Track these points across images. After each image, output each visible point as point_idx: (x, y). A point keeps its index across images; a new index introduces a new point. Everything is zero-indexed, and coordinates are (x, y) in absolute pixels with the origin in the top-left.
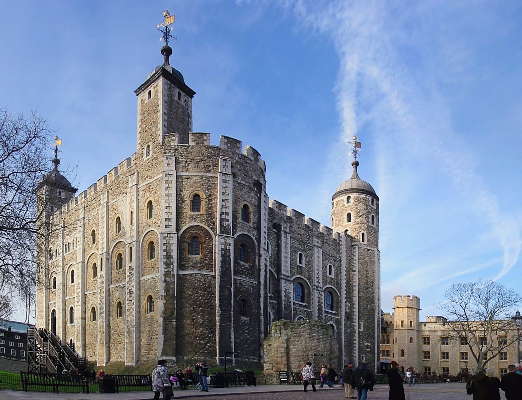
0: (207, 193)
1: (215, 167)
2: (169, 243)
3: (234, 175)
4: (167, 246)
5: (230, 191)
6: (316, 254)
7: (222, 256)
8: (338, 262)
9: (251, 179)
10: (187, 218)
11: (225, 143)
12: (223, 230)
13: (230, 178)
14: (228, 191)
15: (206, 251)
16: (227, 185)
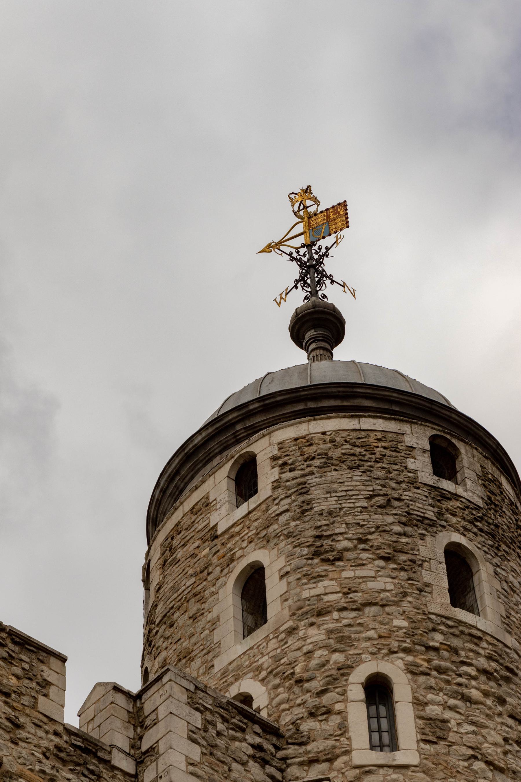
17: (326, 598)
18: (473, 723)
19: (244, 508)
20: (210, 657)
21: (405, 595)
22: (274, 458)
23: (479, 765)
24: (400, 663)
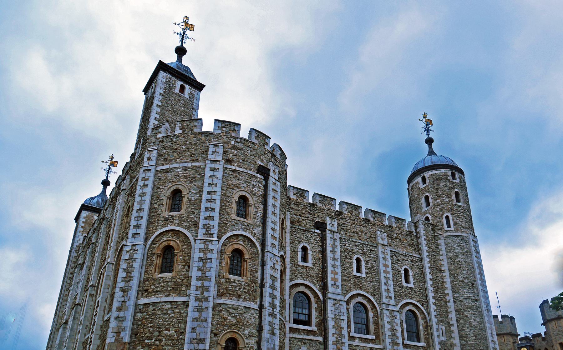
4: (129, 263)
6: (381, 256)
8: (417, 262)
9: (254, 164)
13: (220, 165)
14: (215, 181)
16: (216, 174)
17: (439, 203)
18: (461, 221)
19: (424, 186)
20: (421, 209)
21: (450, 202)
22: (428, 178)
23: (462, 228)
24: (450, 213)
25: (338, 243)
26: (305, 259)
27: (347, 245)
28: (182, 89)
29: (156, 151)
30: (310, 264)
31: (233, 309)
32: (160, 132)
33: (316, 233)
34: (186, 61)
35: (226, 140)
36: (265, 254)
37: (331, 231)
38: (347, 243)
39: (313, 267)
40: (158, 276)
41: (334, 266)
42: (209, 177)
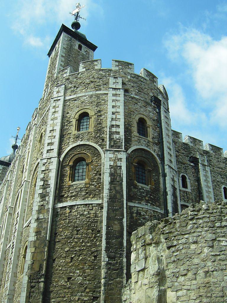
0: (96, 110)
1: (105, 86)
2: (47, 170)
3: (126, 91)
5: (121, 104)
7: (111, 175)
9: (147, 95)
10: (70, 139)
11: (116, 65)
12: (112, 144)
13: (122, 92)
14: (118, 104)
15: (92, 174)
16: (118, 98)
25: (209, 174)
26: (185, 185)
27: (216, 177)
28: (80, 47)
29: (64, 86)
30: (189, 190)
31: (144, 211)
32: (66, 73)
33: (191, 166)
34: (80, 31)
35: (123, 75)
36: (166, 167)
37: (204, 165)
38: (215, 175)
39: (191, 192)
40: (72, 184)
41: (208, 192)
42: (113, 101)
